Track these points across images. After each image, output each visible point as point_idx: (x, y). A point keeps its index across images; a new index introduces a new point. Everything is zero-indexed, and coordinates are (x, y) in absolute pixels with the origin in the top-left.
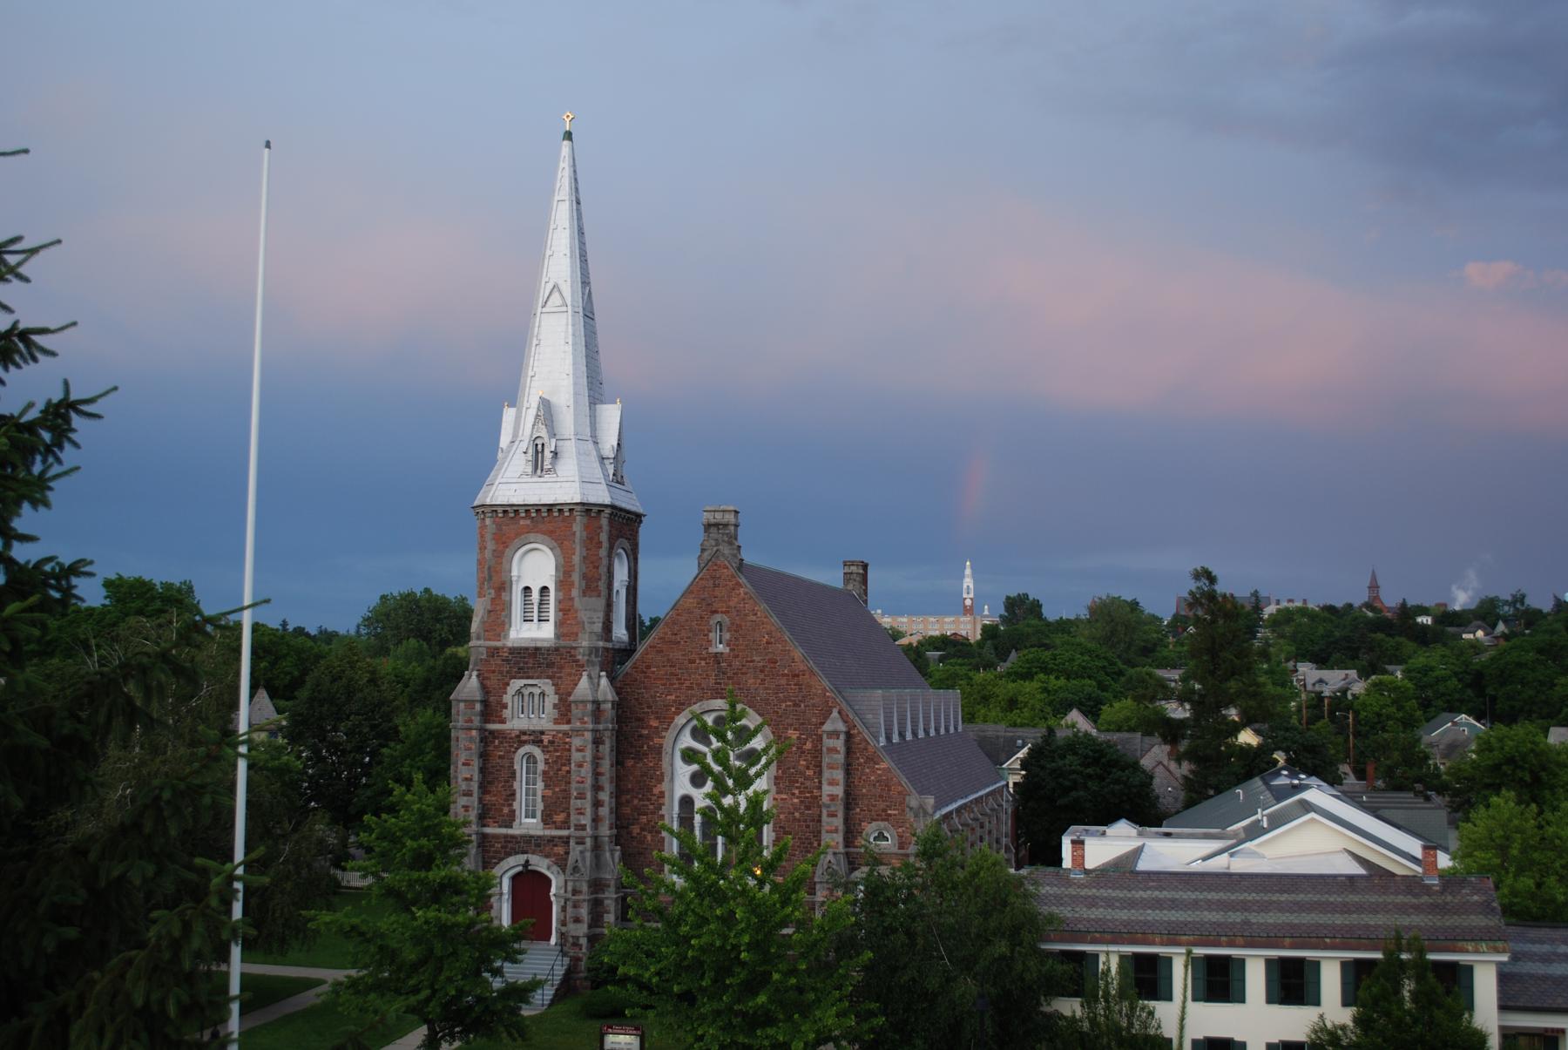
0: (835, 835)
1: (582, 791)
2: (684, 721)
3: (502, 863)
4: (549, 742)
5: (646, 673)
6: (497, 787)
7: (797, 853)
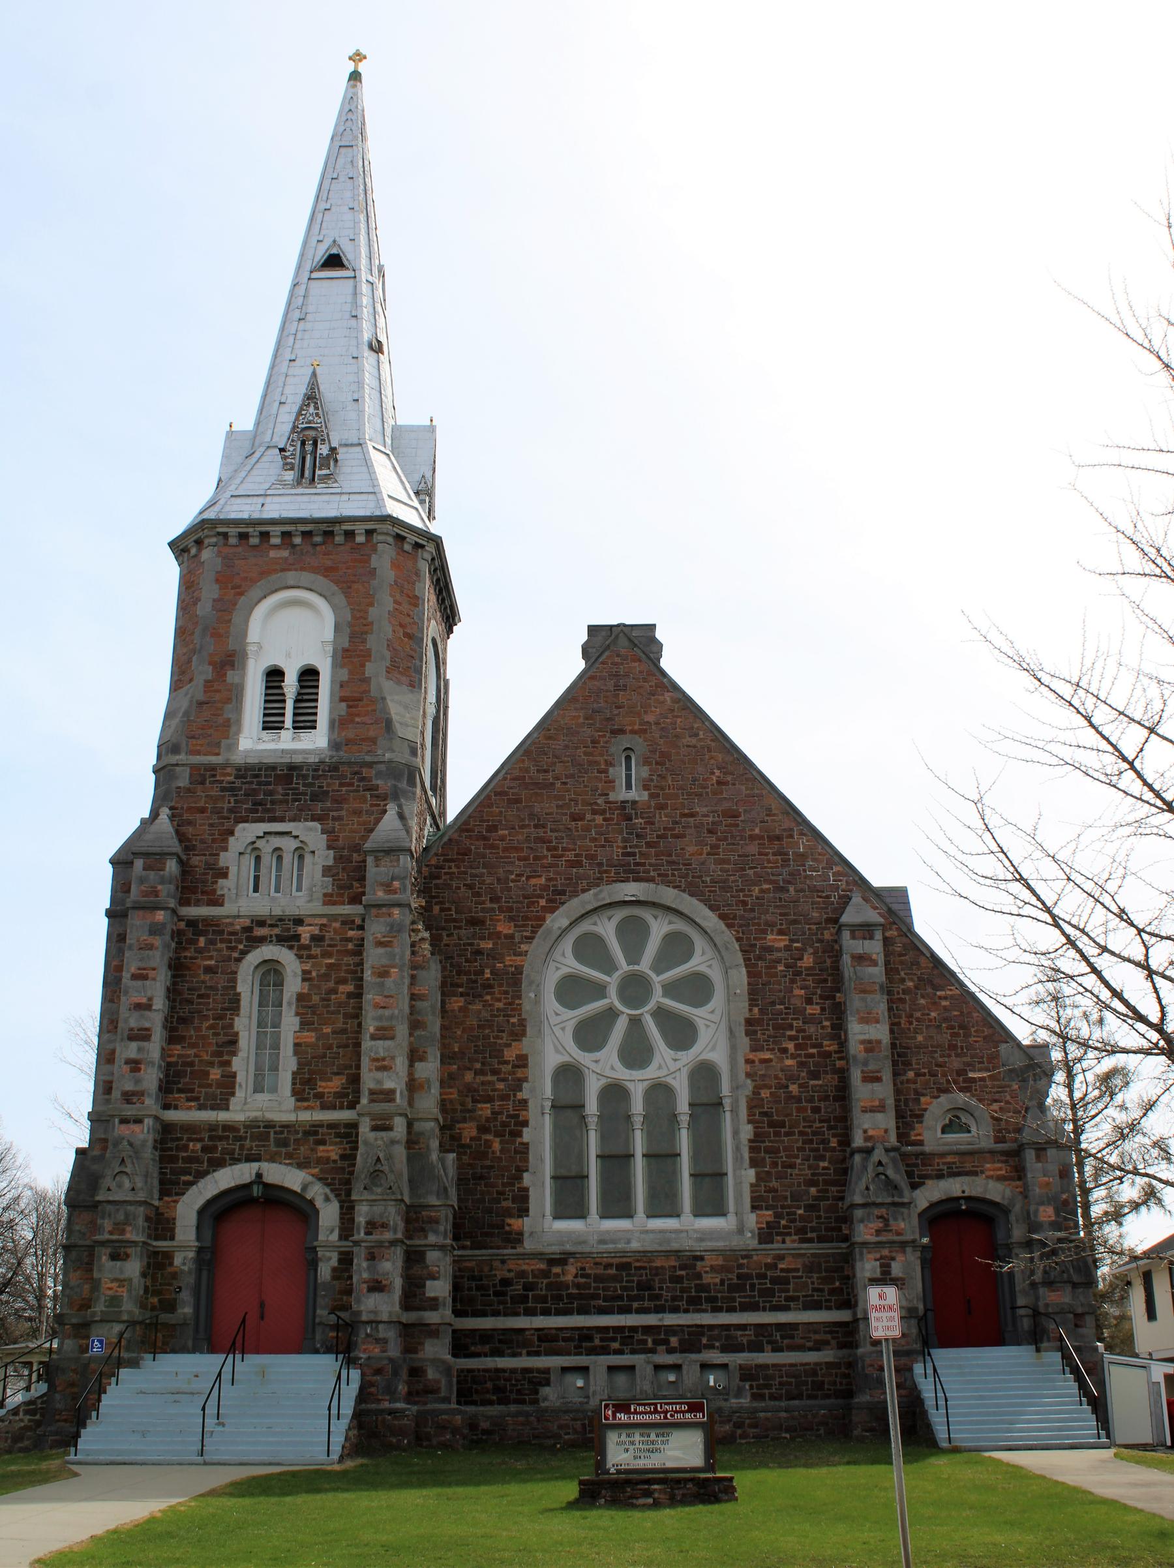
0: (879, 1116)
1: (385, 1024)
2: (565, 922)
3: (202, 1183)
4: (314, 938)
5: (485, 838)
6: (198, 1029)
7: (799, 1161)
